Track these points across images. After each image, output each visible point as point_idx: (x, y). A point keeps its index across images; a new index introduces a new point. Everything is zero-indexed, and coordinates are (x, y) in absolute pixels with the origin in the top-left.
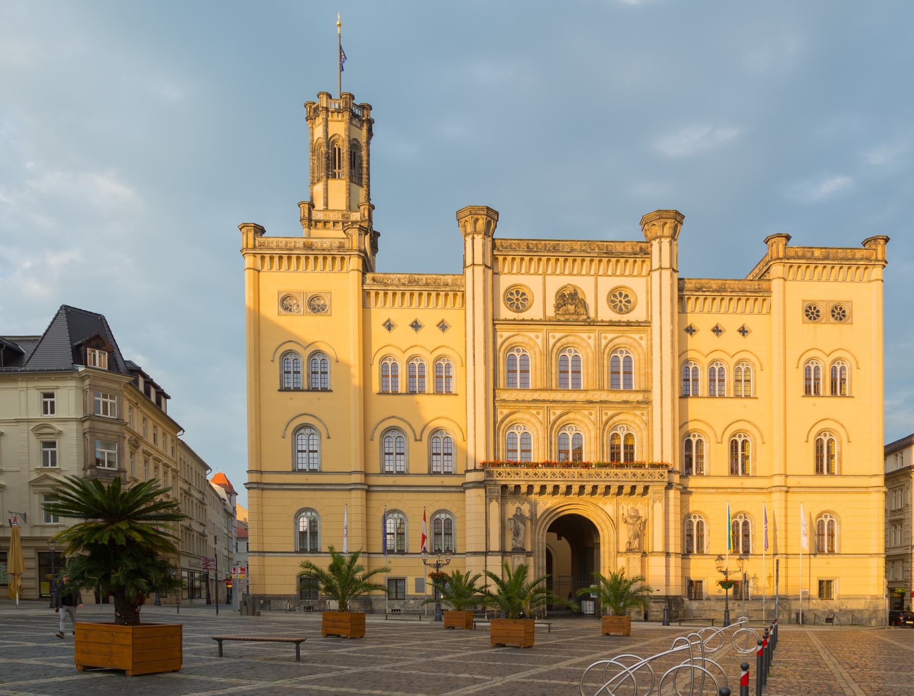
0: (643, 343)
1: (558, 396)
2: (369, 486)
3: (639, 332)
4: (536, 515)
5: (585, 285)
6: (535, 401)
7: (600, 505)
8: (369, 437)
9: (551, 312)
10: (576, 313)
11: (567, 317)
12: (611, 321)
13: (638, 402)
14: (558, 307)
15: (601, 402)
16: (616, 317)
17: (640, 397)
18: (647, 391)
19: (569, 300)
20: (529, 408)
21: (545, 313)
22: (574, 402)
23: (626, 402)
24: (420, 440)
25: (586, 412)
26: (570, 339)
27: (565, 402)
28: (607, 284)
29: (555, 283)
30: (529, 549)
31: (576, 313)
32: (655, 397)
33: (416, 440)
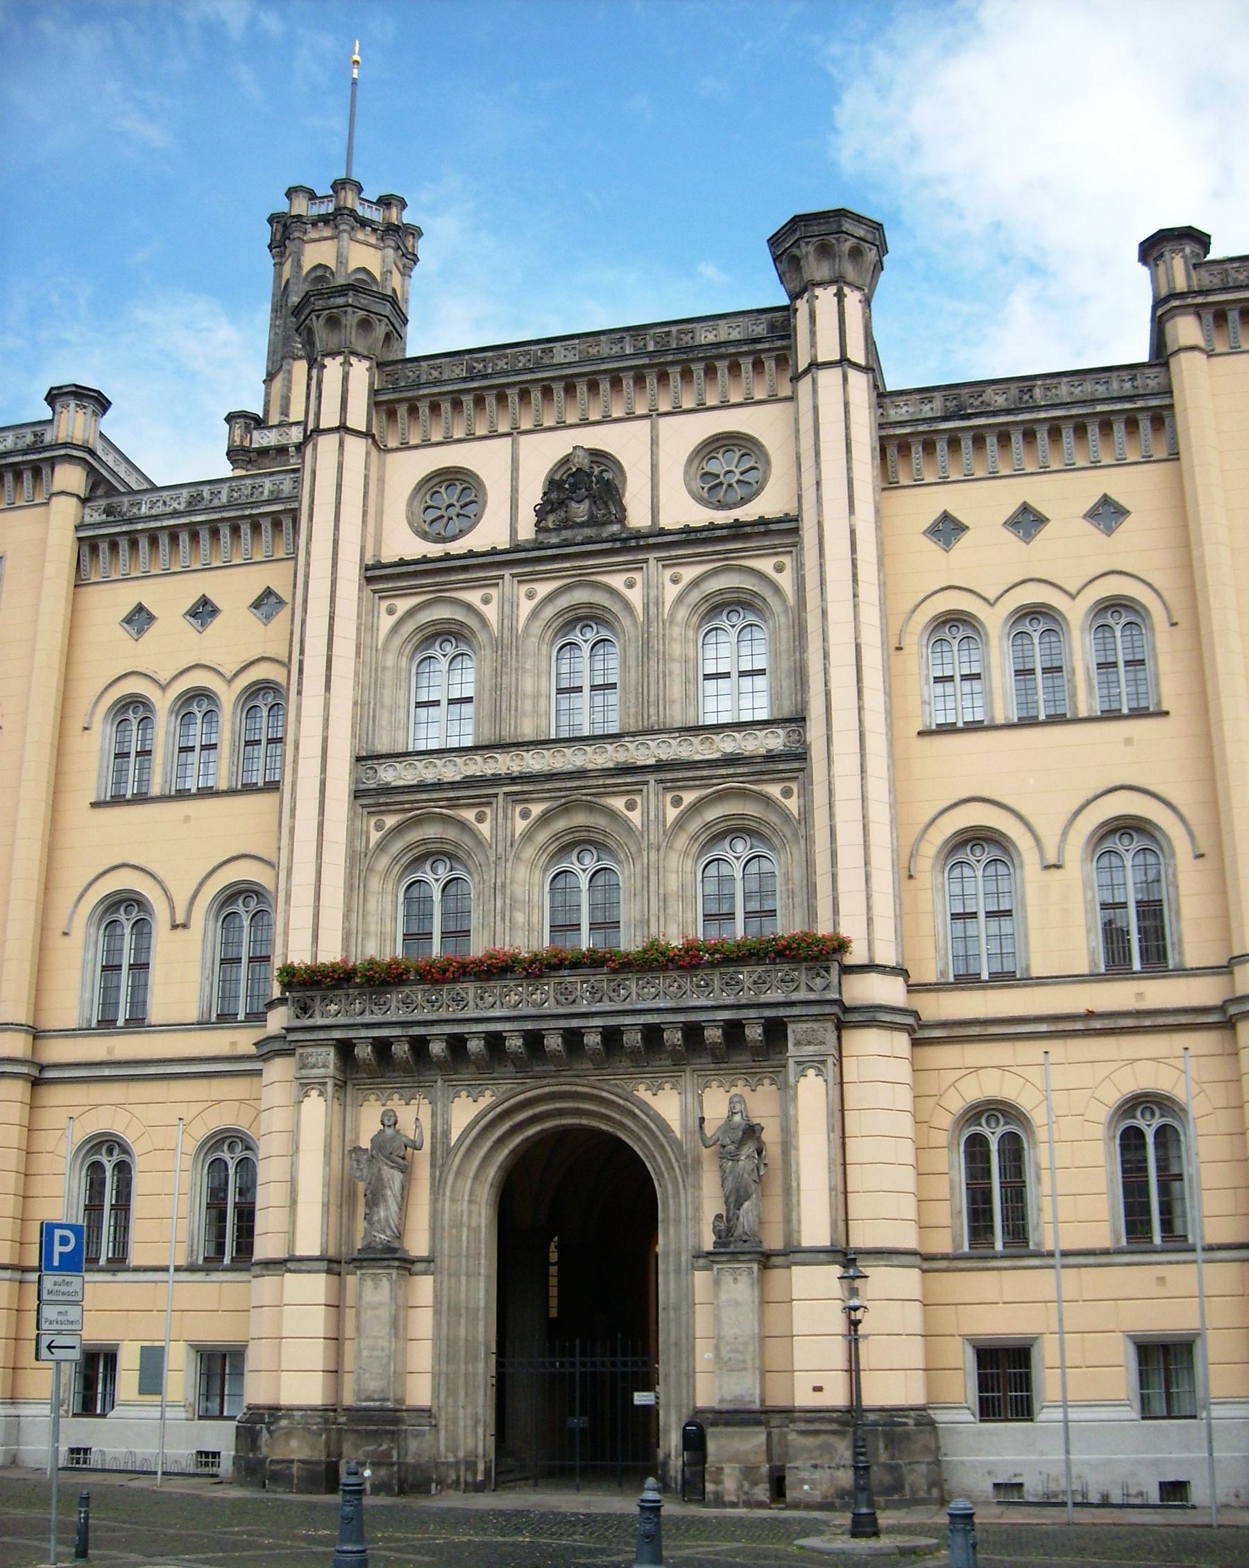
0: (785, 581)
1: (534, 762)
2: (43, 1068)
3: (773, 551)
4: (446, 1134)
5: (623, 441)
6: (469, 782)
7: (643, 1094)
8: (58, 923)
9: (526, 532)
10: (592, 522)
11: (566, 534)
12: (687, 530)
13: (770, 757)
14: (541, 512)
15: (660, 767)
16: (700, 516)
17: (775, 741)
18: (798, 720)
19: (584, 490)
20: (454, 803)
21: (513, 531)
22: (581, 774)
23: (731, 760)
24: (185, 926)
25: (618, 803)
26: (581, 596)
27: (551, 776)
28: (685, 434)
29: (543, 453)
30: (418, 1244)
31: (592, 522)
32: (815, 732)
33: (175, 927)
